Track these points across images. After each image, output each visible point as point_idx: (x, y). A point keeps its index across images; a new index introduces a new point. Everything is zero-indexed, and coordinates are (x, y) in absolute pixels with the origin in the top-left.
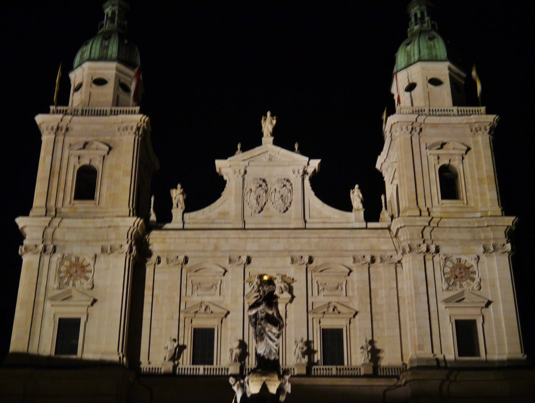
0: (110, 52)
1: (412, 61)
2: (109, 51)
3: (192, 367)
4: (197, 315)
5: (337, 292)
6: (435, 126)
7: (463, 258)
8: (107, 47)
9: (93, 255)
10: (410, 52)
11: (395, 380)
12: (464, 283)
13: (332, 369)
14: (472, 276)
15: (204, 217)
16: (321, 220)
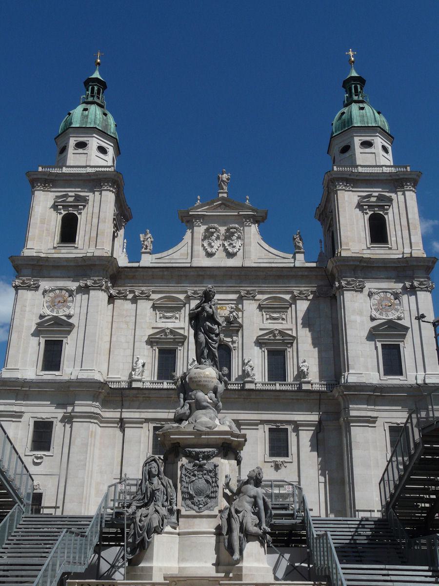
0: (89, 121)
1: (347, 128)
5: (280, 321)
8: (87, 116)
12: (390, 313)
13: (275, 385)
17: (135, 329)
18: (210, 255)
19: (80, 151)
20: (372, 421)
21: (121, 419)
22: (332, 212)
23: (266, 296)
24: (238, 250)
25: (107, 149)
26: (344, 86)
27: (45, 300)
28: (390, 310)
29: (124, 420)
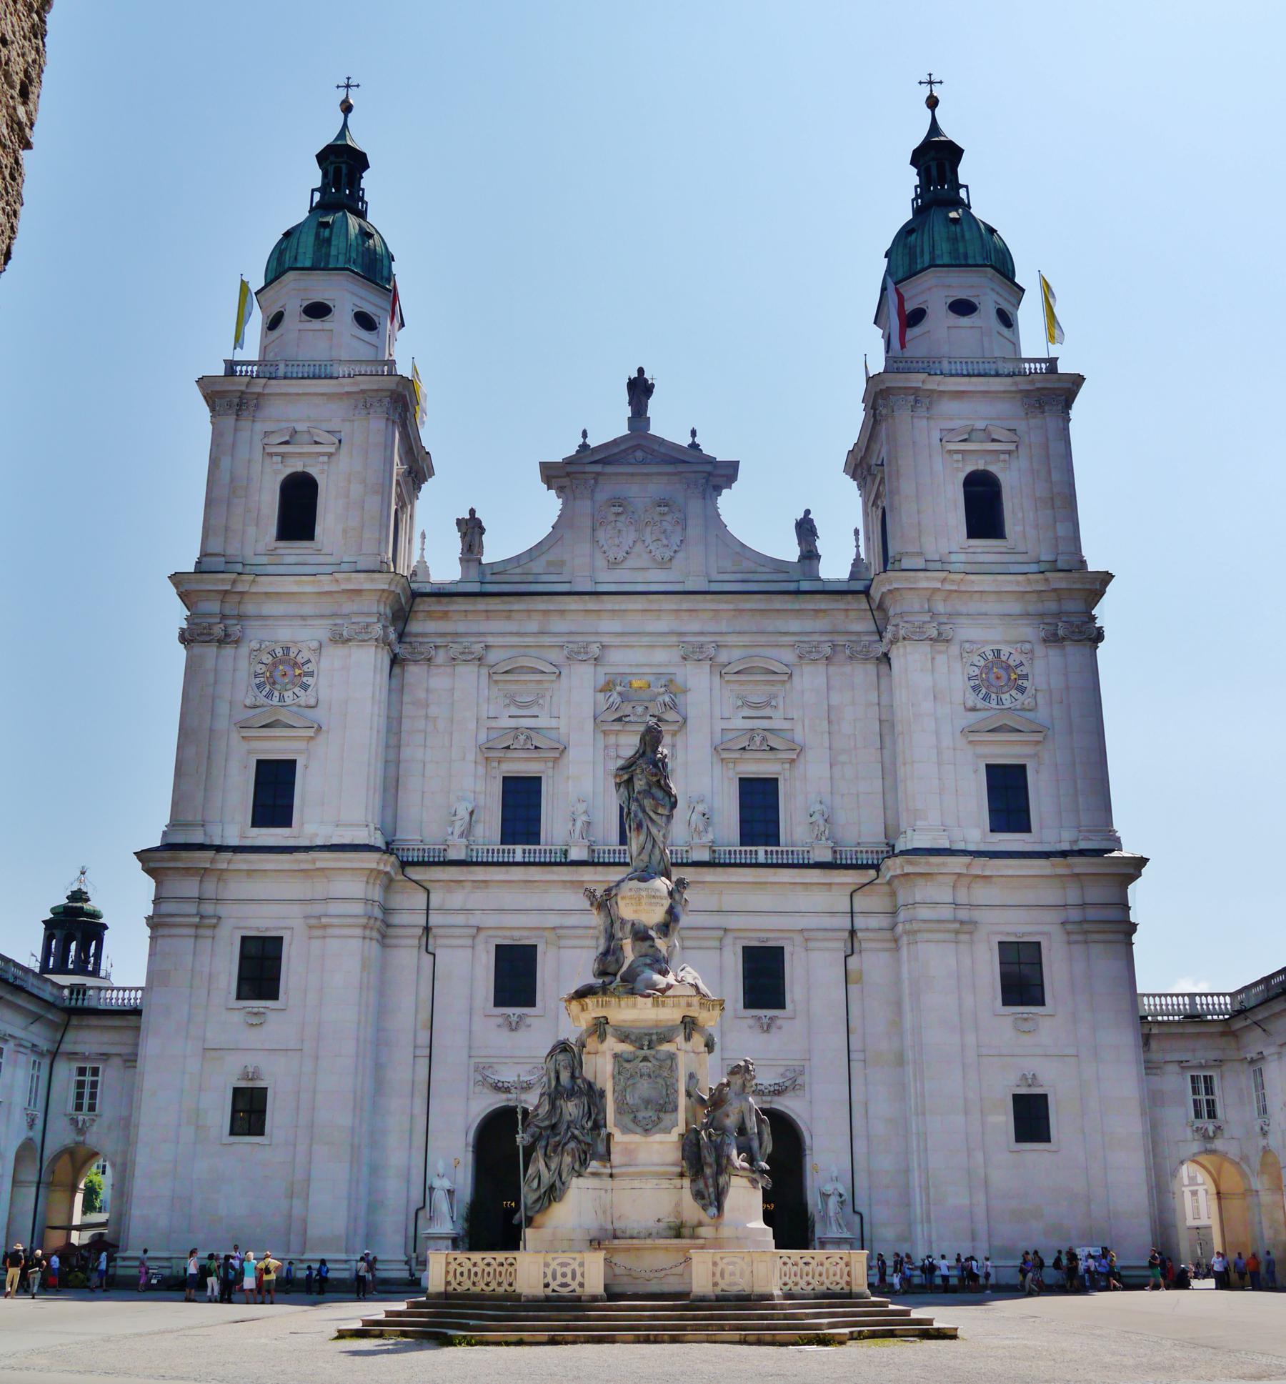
0: (333, 252)
1: (919, 267)
2: (333, 248)
3: (502, 847)
4: (510, 754)
5: (767, 712)
6: (959, 395)
7: (1006, 650)
8: (328, 241)
9: (315, 645)
10: (915, 246)
11: (872, 873)
12: (1005, 697)
14: (1020, 682)
15: (518, 570)
16: (739, 577)
17: (451, 734)
18: (614, 564)
19: (316, 324)
20: (964, 928)
21: (427, 929)
22: (882, 465)
23: (737, 654)
24: (672, 554)
25: (376, 319)
26: (913, 163)
27: (252, 671)
28: (1006, 689)
29: (434, 931)
